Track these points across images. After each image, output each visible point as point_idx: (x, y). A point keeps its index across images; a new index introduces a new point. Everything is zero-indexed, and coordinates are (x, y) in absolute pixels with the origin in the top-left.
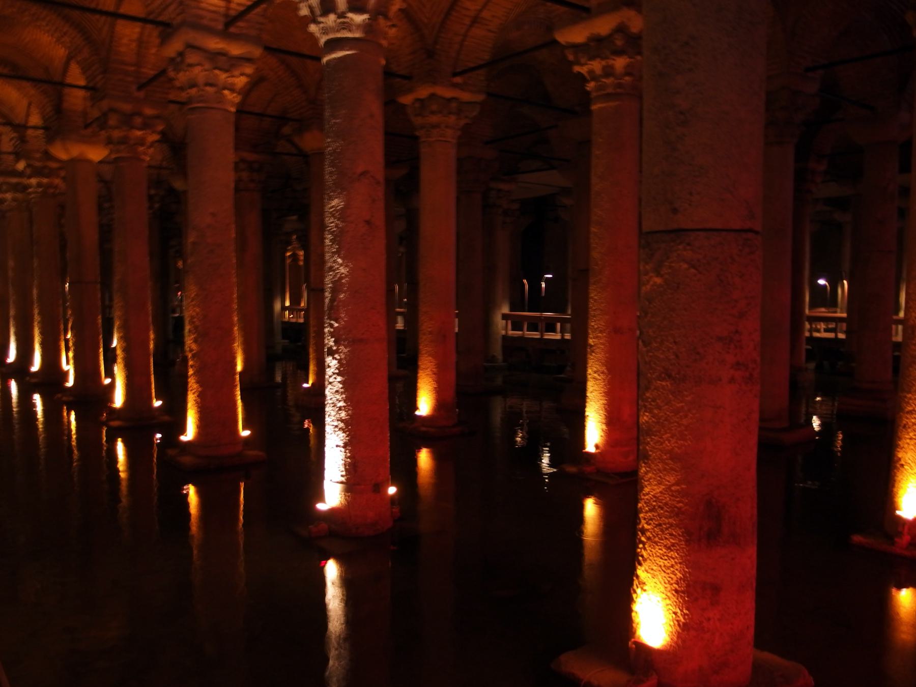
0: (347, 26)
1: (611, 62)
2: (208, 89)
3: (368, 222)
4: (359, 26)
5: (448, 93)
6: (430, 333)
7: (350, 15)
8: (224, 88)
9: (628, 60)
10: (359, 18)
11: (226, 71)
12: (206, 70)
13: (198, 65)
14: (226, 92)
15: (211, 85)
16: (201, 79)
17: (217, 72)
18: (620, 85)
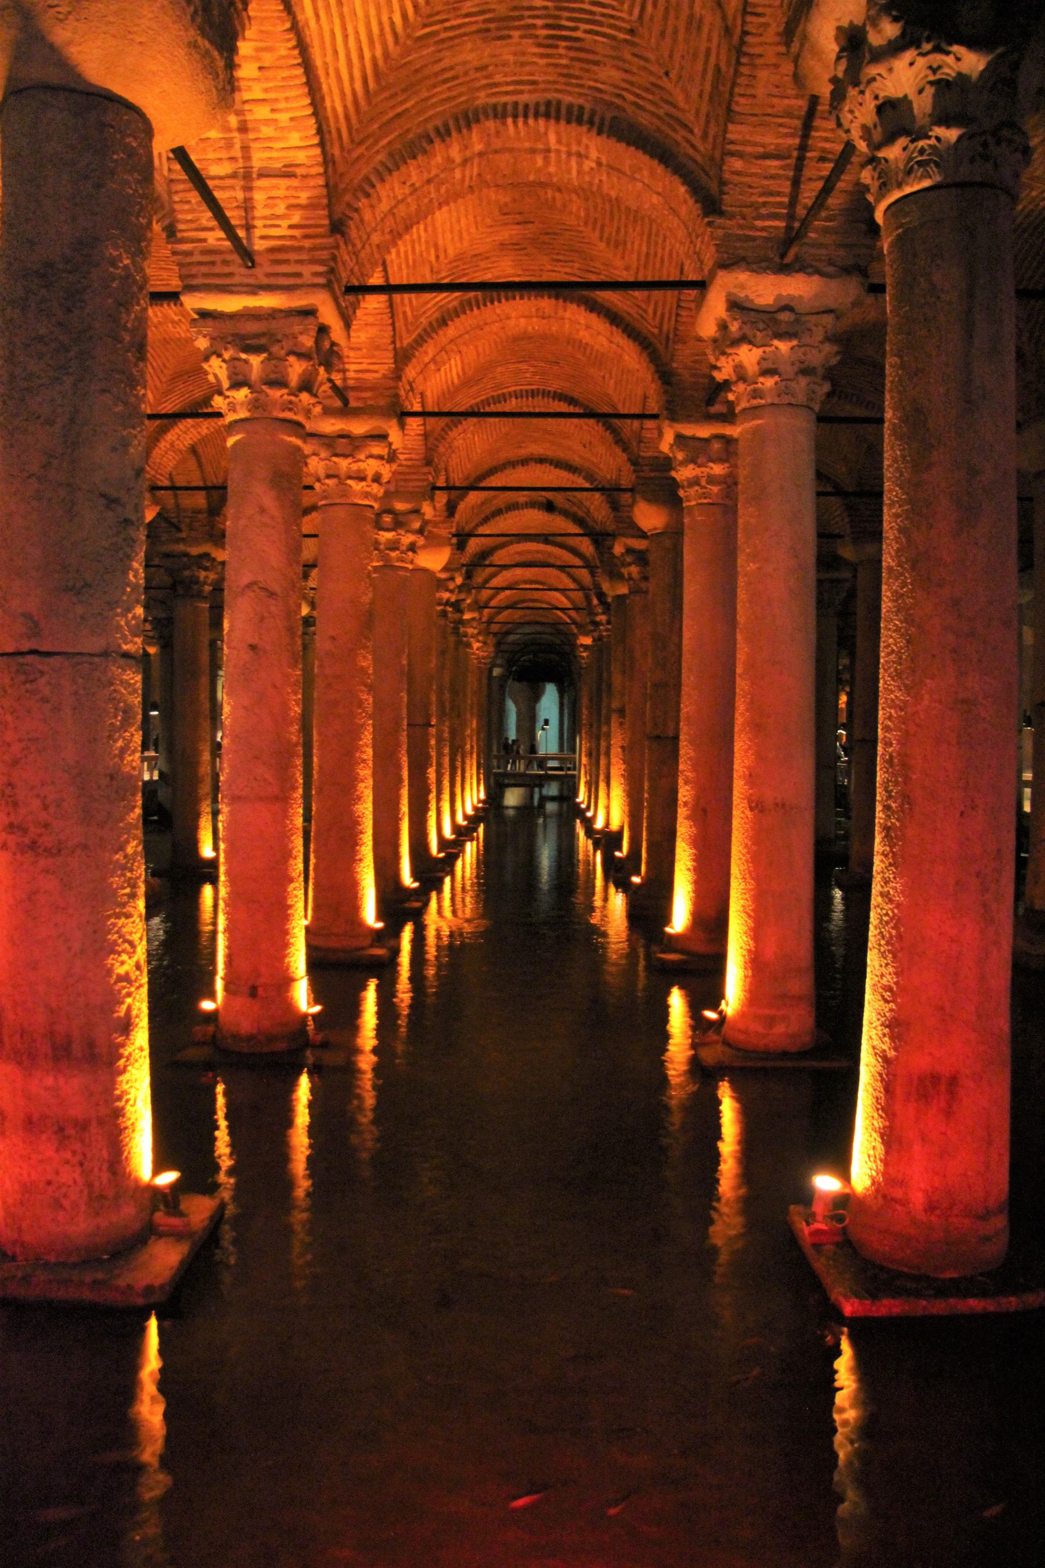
0: (232, 407)
1: (737, 359)
2: (327, 481)
3: (253, 647)
4: (242, 404)
5: (704, 431)
6: (685, 804)
7: (228, 393)
8: (350, 478)
9: (757, 352)
10: (243, 394)
11: (345, 456)
12: (322, 460)
13: (315, 454)
14: (350, 482)
15: (328, 477)
16: (322, 473)
17: (335, 459)
18: (756, 394)
